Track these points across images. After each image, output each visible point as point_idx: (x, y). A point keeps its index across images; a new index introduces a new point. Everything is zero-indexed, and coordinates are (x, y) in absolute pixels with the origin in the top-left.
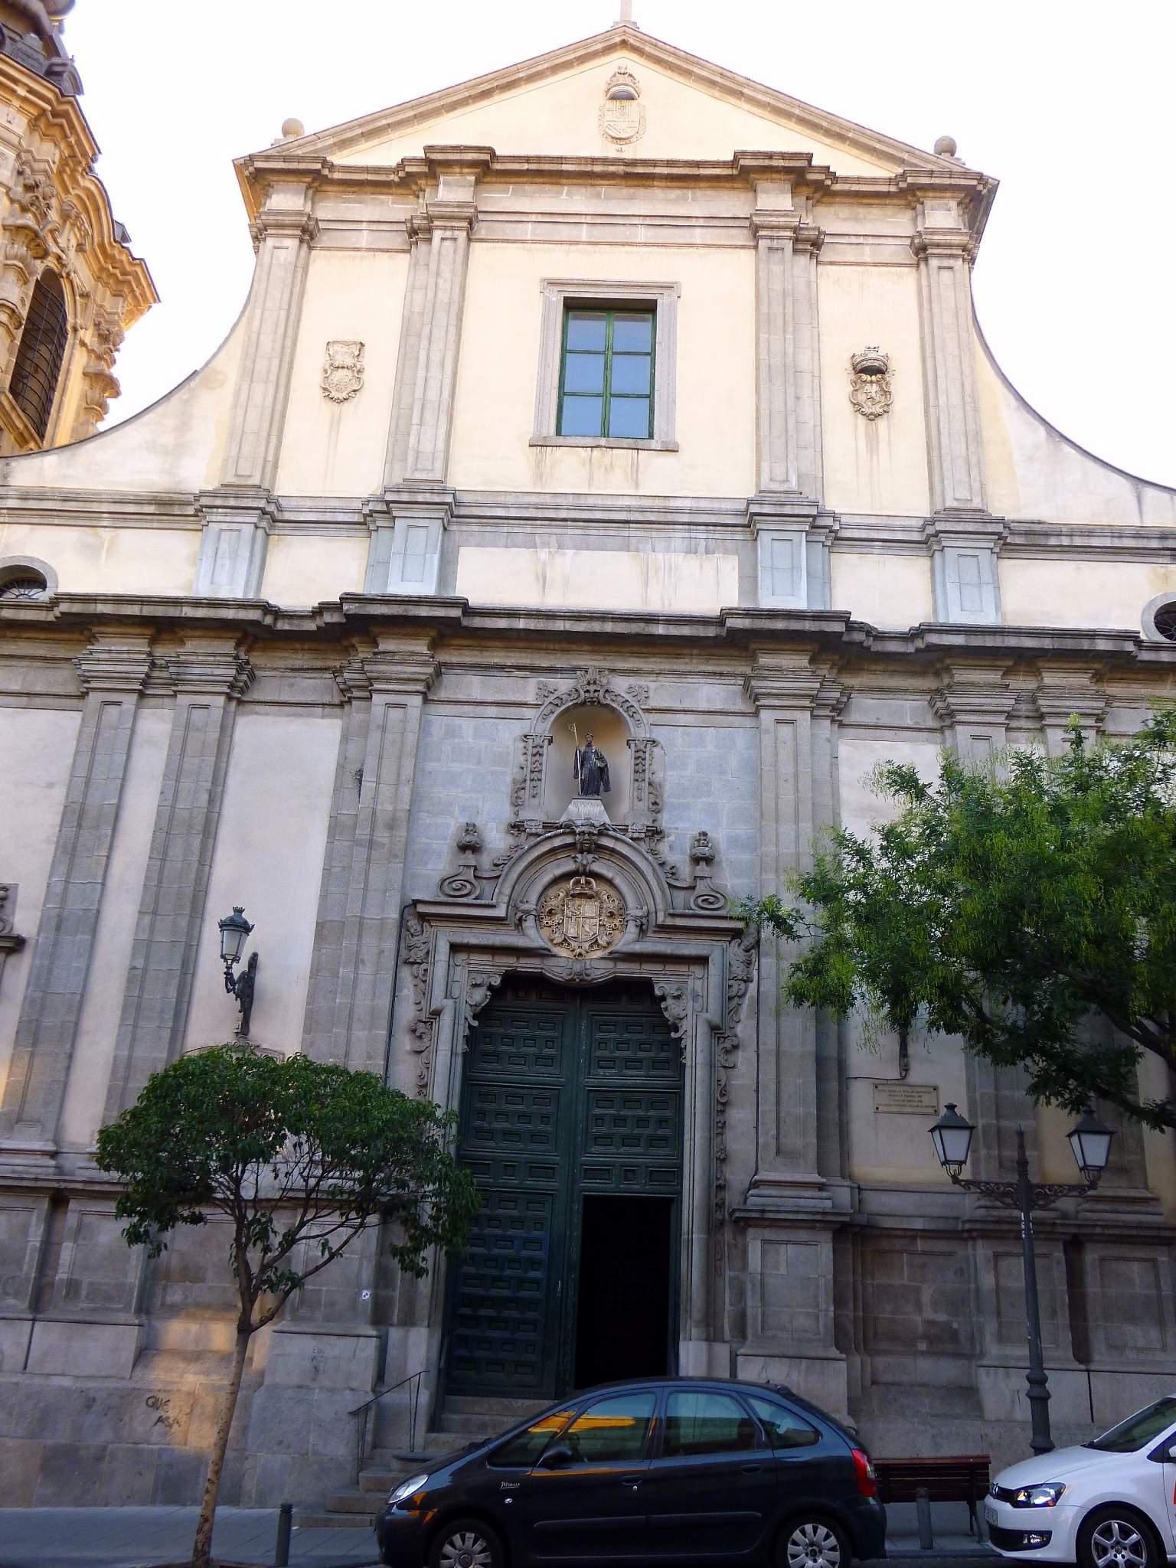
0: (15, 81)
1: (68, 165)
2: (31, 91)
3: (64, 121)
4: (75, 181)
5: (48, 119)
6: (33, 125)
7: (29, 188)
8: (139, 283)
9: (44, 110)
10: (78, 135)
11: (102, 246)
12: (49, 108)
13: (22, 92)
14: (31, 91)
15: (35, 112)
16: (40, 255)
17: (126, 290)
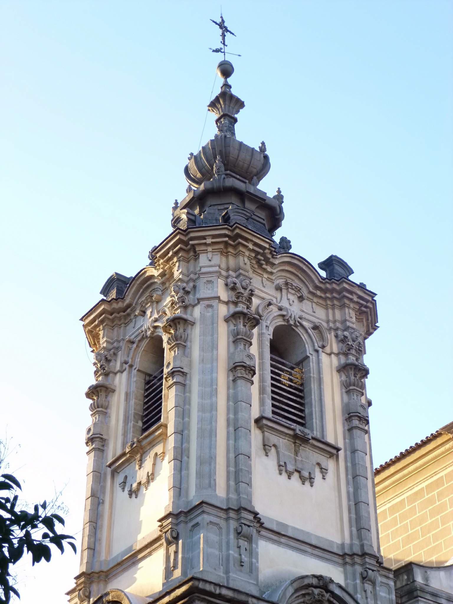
0: (204, 238)
1: (260, 260)
2: (214, 236)
3: (240, 240)
4: (273, 264)
5: (231, 245)
6: (225, 254)
7: (234, 289)
8: (351, 293)
9: (226, 243)
10: (252, 241)
11: (317, 288)
12: (227, 239)
13: (209, 241)
14: (214, 236)
15: (222, 246)
16: (255, 323)
17: (346, 301)
